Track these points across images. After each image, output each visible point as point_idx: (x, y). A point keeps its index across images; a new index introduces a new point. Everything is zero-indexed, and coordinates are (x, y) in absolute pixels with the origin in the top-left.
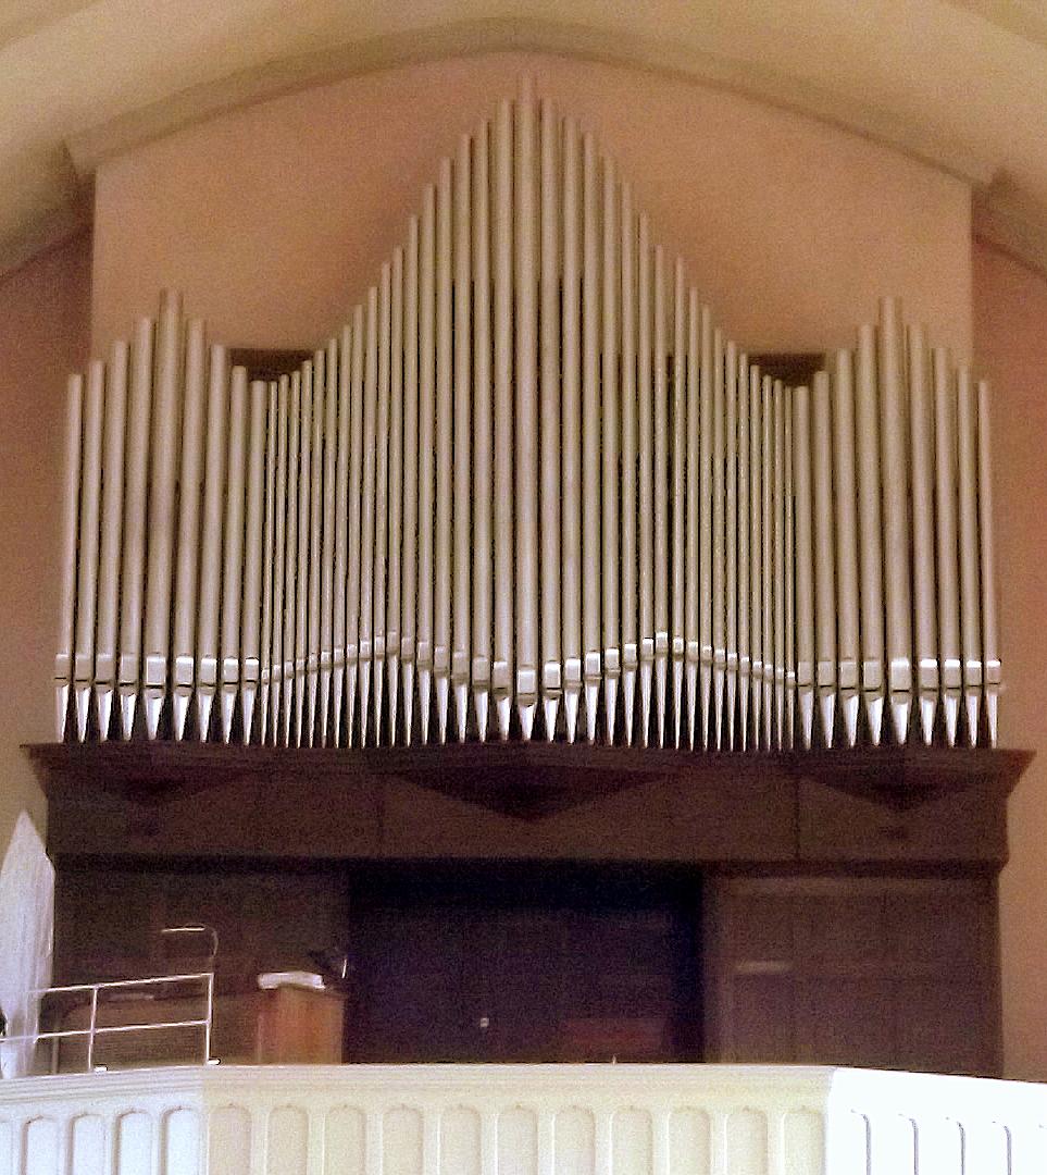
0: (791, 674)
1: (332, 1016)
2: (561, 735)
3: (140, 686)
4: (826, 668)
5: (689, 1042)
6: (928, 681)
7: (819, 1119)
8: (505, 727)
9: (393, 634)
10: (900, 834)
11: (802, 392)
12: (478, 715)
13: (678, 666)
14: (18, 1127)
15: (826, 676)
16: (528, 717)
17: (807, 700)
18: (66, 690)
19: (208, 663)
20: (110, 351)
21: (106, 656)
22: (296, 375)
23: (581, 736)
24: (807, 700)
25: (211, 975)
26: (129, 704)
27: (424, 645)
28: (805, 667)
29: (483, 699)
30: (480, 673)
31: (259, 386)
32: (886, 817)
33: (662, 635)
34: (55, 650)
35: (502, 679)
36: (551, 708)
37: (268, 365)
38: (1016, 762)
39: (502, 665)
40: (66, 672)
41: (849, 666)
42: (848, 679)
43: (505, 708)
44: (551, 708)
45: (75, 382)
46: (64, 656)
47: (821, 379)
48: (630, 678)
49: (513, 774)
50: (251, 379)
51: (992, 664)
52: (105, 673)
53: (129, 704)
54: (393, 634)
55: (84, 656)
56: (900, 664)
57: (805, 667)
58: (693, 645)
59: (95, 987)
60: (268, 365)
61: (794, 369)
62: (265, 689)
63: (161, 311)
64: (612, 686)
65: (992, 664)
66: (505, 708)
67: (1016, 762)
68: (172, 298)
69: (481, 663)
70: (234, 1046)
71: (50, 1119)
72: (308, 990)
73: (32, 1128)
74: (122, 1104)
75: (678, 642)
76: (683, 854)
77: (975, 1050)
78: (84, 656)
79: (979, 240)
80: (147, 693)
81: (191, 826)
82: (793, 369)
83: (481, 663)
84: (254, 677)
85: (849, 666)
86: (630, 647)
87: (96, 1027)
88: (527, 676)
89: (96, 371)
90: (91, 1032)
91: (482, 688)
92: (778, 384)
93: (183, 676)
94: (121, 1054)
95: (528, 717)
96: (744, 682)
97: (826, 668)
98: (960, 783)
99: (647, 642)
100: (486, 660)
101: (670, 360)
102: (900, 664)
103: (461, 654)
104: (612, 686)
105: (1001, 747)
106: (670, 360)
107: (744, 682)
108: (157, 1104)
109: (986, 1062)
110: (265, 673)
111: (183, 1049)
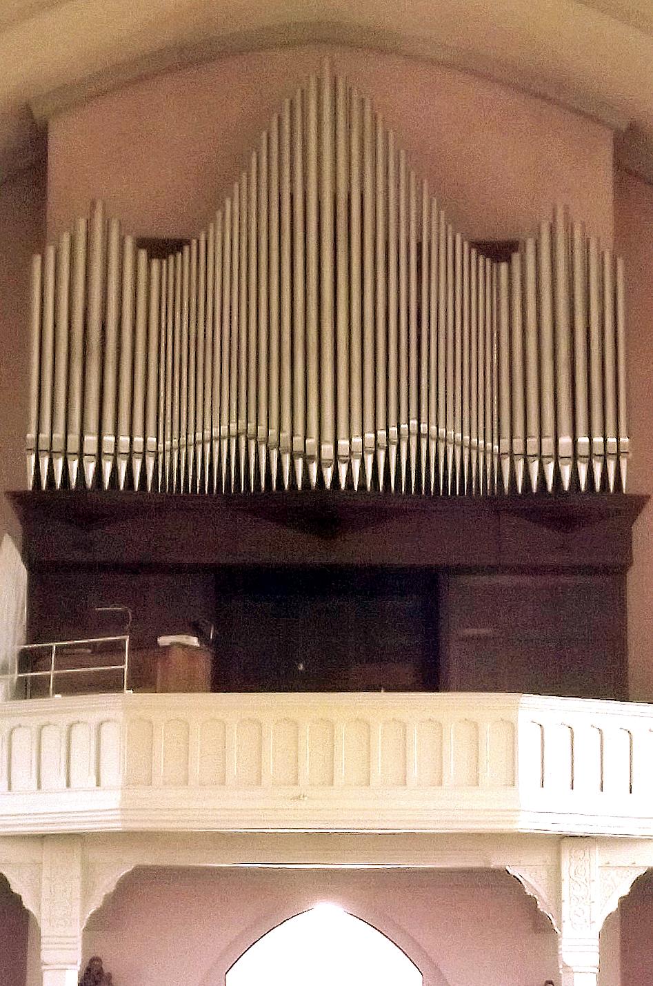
0: (496, 447)
1: (204, 665)
3: (81, 454)
4: (519, 442)
5: (430, 678)
7: (513, 727)
8: (314, 481)
11: (504, 266)
12: (296, 473)
15: (518, 448)
16: (328, 474)
17: (506, 463)
18: (33, 457)
19: (124, 440)
20: (59, 240)
21: (59, 435)
22: (179, 255)
23: (362, 486)
24: (506, 463)
25: (127, 638)
26: (74, 466)
28: (505, 442)
29: (299, 463)
31: (155, 264)
33: (414, 422)
34: (27, 431)
37: (161, 248)
39: (312, 441)
40: (33, 446)
41: (533, 442)
42: (532, 450)
43: (314, 469)
44: (343, 469)
45: (37, 259)
46: (32, 435)
47: (516, 258)
48: (393, 449)
49: (320, 510)
50: (150, 257)
51: (624, 440)
52: (58, 447)
53: (74, 466)
55: (45, 435)
56: (565, 440)
57: (505, 442)
58: (433, 428)
59: (54, 645)
60: (161, 248)
61: (499, 251)
62: (161, 457)
63: (92, 216)
64: (382, 454)
65: (624, 440)
66: (314, 469)
68: (99, 206)
69: (298, 439)
70: (143, 681)
72: (192, 647)
74: (71, 718)
75: (424, 426)
76: (425, 561)
77: (610, 683)
78: (45, 435)
79: (618, 166)
81: (111, 543)
82: (499, 251)
83: (298, 439)
84: (154, 449)
85: (533, 442)
86: (393, 430)
87: (55, 669)
88: (328, 450)
89: (51, 251)
90: (52, 673)
92: (488, 260)
93: (108, 449)
94: (70, 686)
95: (328, 474)
96: (466, 452)
97: (519, 442)
98: (603, 516)
99: (404, 426)
101: (419, 246)
102: (565, 440)
104: (382, 454)
105: (632, 492)
106: (419, 246)
107: (466, 452)
108: (94, 718)
110: (161, 446)
111: (110, 684)
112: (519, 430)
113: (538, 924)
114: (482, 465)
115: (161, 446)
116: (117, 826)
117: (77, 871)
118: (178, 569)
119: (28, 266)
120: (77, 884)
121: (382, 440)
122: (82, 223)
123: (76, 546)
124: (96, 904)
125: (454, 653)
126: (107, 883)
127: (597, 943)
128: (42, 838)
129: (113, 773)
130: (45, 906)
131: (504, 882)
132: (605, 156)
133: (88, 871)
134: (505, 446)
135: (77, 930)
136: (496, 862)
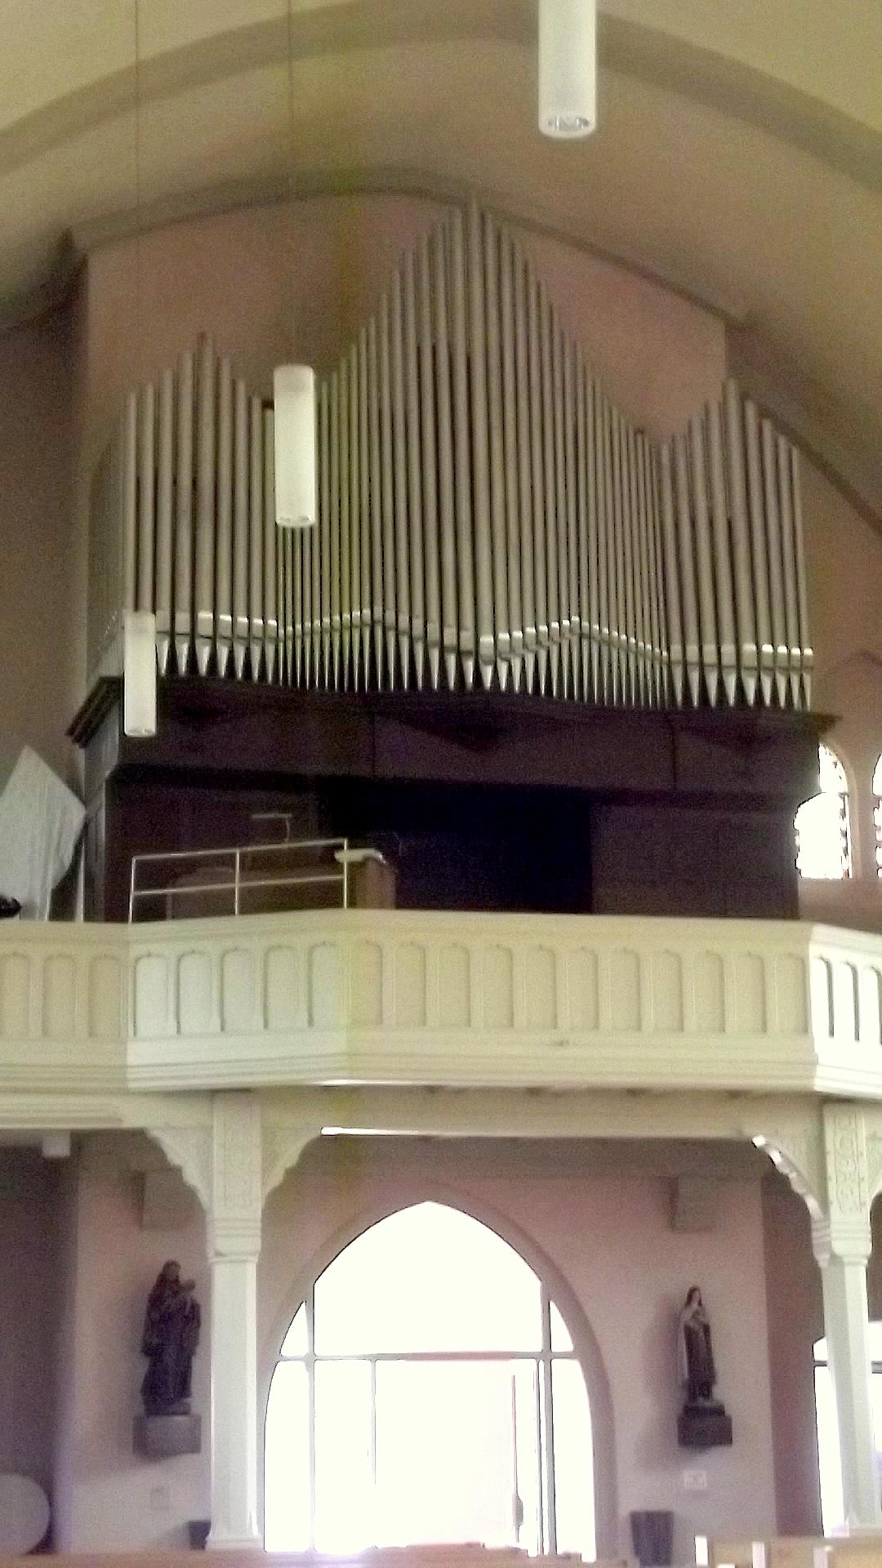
0: (665, 653)
1: (389, 886)
3: (193, 635)
7: (803, 965)
8: (470, 679)
9: (378, 610)
13: (585, 643)
14: (173, 960)
16: (488, 673)
28: (676, 648)
29: (451, 661)
35: (467, 642)
43: (469, 666)
44: (503, 669)
49: (473, 715)
54: (378, 610)
57: (676, 648)
59: (238, 852)
66: (469, 666)
71: (201, 953)
73: (228, 958)
76: (590, 782)
80: (198, 642)
85: (710, 649)
88: (487, 640)
91: (451, 650)
94: (258, 903)
100: (454, 630)
105: (818, 710)
110: (281, 631)
115: (281, 631)
120: (256, 1156)
124: (277, 1177)
126: (290, 1156)
127: (259, 1225)
128: (213, 1094)
130: (217, 1181)
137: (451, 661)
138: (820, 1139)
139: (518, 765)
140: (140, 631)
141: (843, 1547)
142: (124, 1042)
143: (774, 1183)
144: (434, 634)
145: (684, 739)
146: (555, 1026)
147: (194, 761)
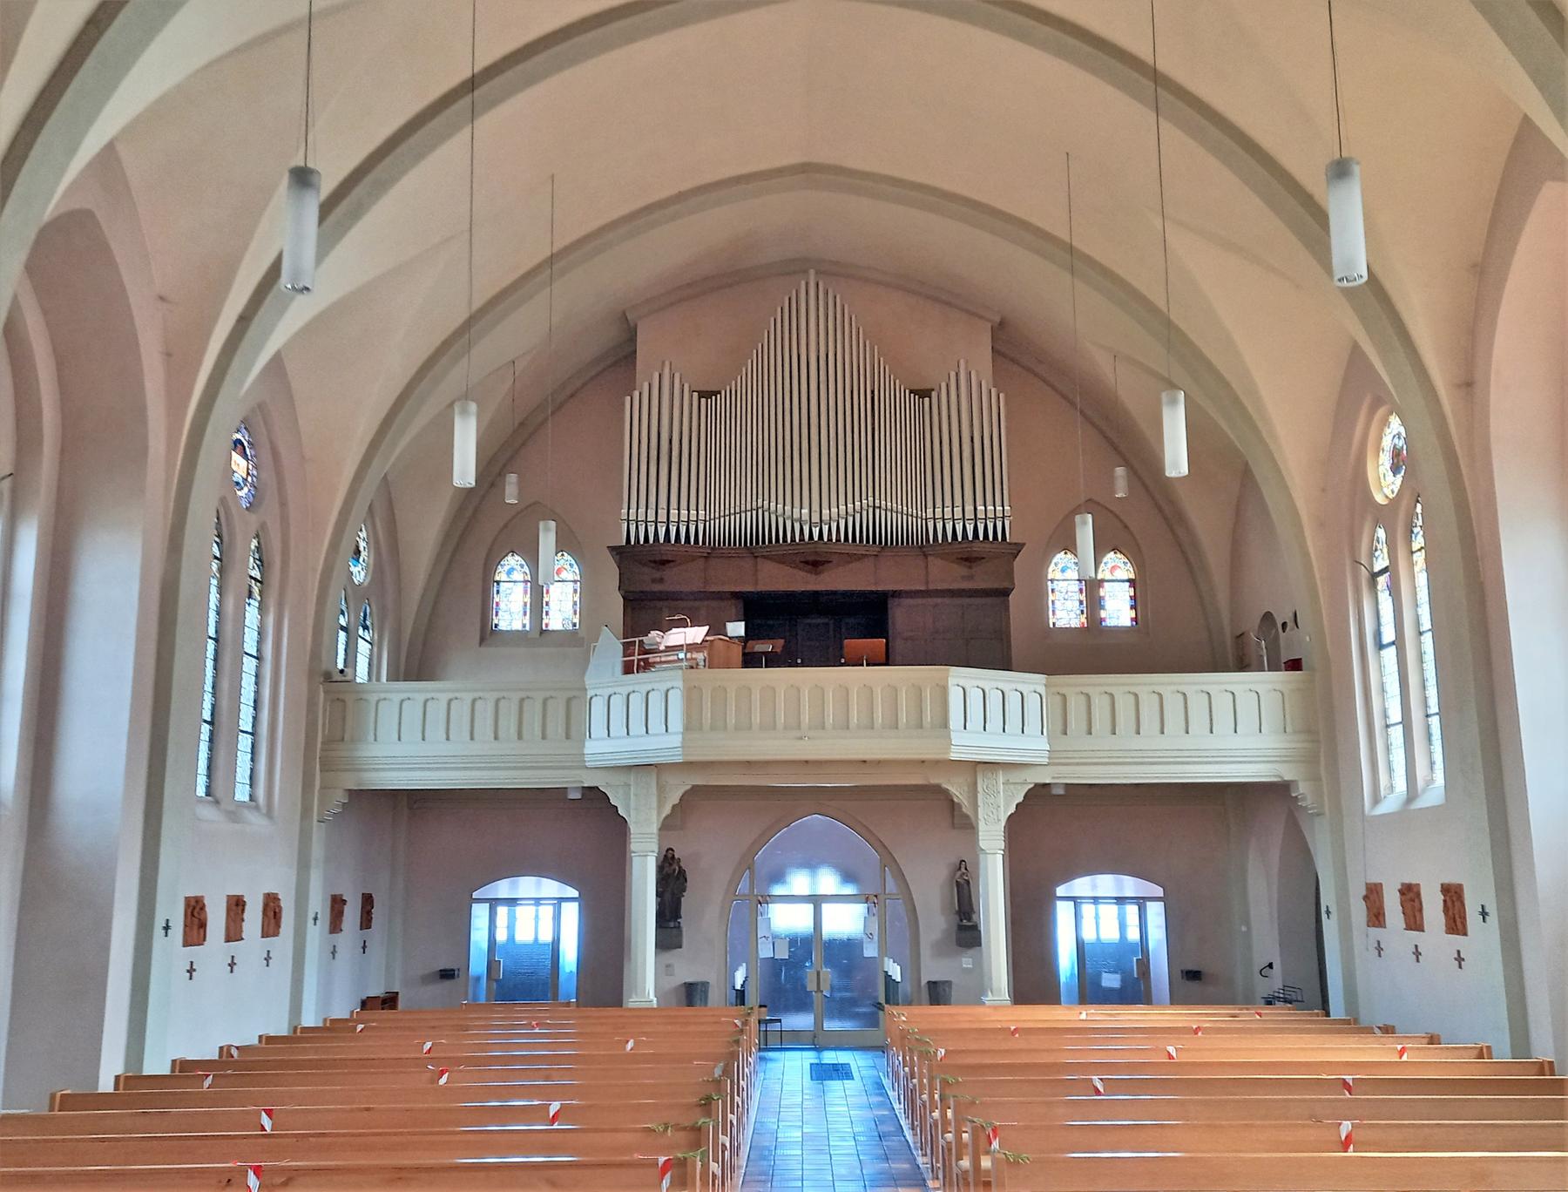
2: (830, 539)
4: (938, 511)
6: (981, 515)
10: (970, 578)
27: (773, 505)
28: (930, 511)
30: (797, 515)
32: (961, 570)
35: (805, 517)
36: (825, 529)
37: (706, 394)
38: (1018, 548)
41: (948, 510)
44: (825, 529)
46: (624, 511)
56: (969, 508)
57: (930, 511)
60: (706, 394)
61: (924, 393)
67: (1018, 548)
81: (679, 579)
82: (924, 393)
83: (796, 511)
85: (948, 510)
89: (636, 394)
93: (673, 518)
102: (969, 508)
103: (788, 508)
109: (1006, 666)
112: (939, 504)
113: (962, 822)
114: (915, 525)
116: (679, 759)
117: (654, 790)
118: (719, 596)
119: (623, 404)
120: (654, 801)
121: (850, 511)
122: (656, 375)
123: (654, 581)
124: (667, 810)
125: (899, 646)
126: (674, 798)
129: (676, 723)
131: (939, 792)
132: (986, 339)
133: (661, 789)
134: (930, 515)
135: (654, 828)
136: (934, 781)
137: (797, 526)
138: (975, 784)
139: (837, 580)
140: (547, 529)
141: (404, 1012)
142: (583, 742)
143: (952, 806)
144: (788, 513)
145: (936, 564)
146: (799, 727)
147: (657, 588)
